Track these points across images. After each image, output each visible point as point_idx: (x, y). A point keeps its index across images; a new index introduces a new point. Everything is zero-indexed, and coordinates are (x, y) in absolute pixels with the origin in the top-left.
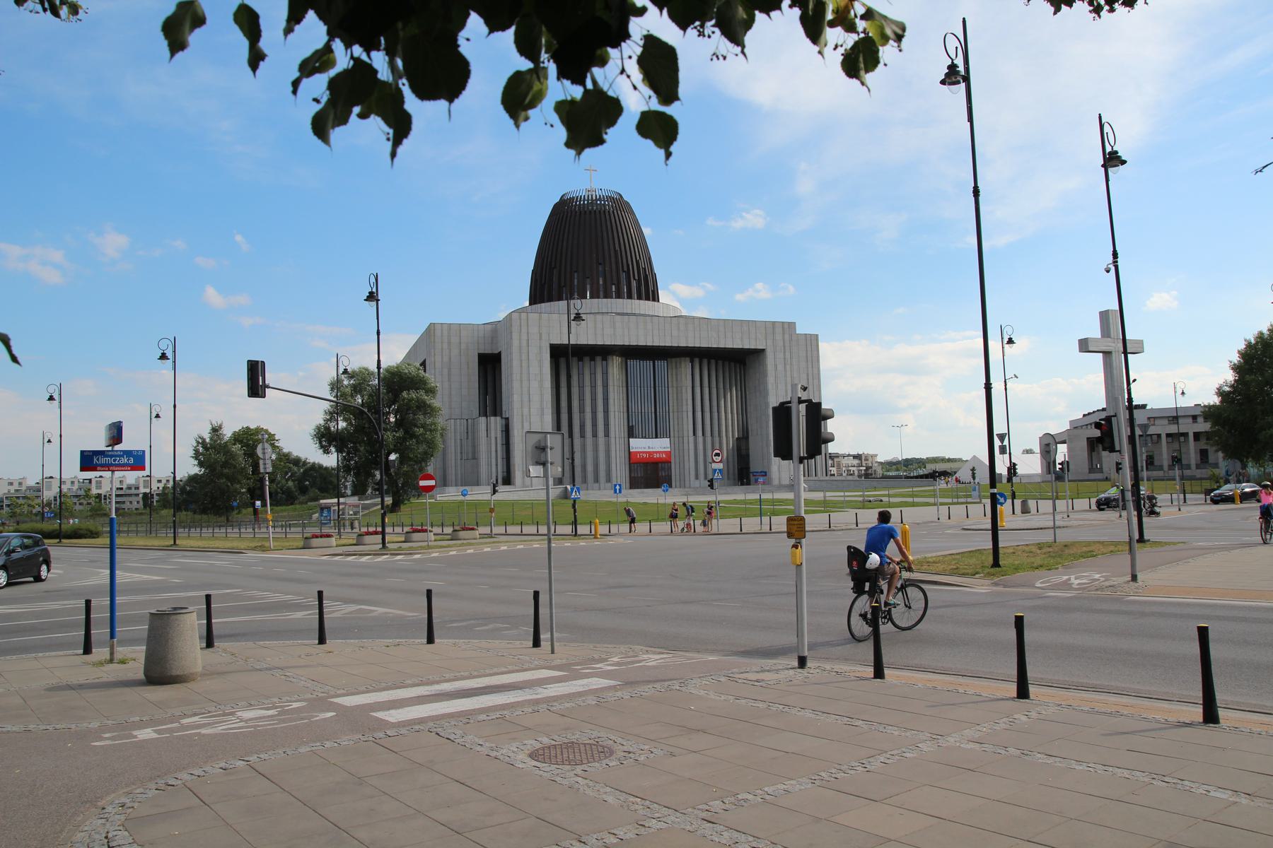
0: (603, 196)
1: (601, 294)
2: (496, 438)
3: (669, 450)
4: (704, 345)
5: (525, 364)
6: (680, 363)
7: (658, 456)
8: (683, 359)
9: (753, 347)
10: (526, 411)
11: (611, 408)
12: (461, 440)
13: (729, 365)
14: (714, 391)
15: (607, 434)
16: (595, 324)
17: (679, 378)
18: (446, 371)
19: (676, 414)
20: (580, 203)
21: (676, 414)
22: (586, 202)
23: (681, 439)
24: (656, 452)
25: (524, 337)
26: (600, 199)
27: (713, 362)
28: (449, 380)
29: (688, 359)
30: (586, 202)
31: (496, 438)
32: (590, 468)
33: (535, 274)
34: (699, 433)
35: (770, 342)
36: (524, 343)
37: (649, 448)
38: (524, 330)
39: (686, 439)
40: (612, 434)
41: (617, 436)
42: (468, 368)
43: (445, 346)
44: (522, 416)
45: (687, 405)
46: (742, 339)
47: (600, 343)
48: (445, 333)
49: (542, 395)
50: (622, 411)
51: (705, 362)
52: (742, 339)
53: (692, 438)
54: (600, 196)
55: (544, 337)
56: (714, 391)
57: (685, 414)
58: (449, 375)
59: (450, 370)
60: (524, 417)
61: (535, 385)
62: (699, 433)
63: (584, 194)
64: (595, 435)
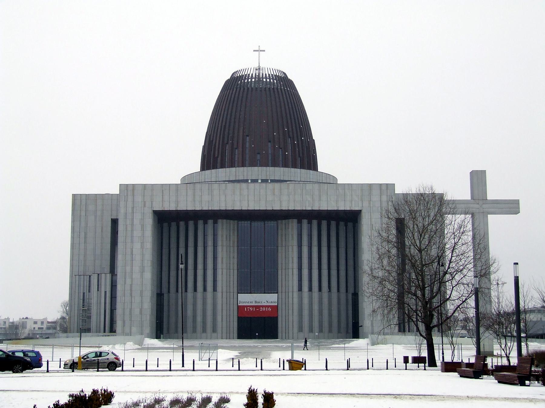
0: (269, 75)
1: (270, 164)
2: (105, 292)
3: (276, 304)
4: (298, 208)
5: (129, 228)
6: (288, 224)
7: (264, 309)
8: (290, 220)
9: (348, 209)
10: (128, 269)
11: (219, 266)
12: (84, 293)
13: (346, 226)
14: (324, 249)
15: (215, 289)
16: (194, 193)
17: (287, 239)
18: (83, 235)
19: (284, 271)
20: (251, 80)
21: (284, 271)
22: (253, 80)
23: (287, 293)
24: (263, 306)
25: (130, 204)
26: (266, 78)
27: (342, 224)
28: (85, 242)
29: (295, 221)
30: (253, 80)
31: (105, 292)
32: (199, 319)
33: (204, 147)
34: (305, 288)
35: (366, 204)
36: (130, 210)
37: (256, 302)
38: (130, 199)
39: (290, 294)
40: (219, 289)
41: (225, 290)
42: (102, 231)
43: (83, 213)
44: (125, 273)
45: (293, 262)
46: (337, 201)
47: (198, 208)
48: (84, 202)
49: (143, 255)
50: (231, 268)
51: (342, 224)
52: (337, 201)
53: (296, 294)
54: (266, 74)
55: (148, 204)
56: (324, 249)
57: (290, 271)
58: (85, 238)
59: (86, 234)
60: (127, 274)
61: (137, 246)
62: (305, 288)
63: (251, 73)
64: (195, 290)
